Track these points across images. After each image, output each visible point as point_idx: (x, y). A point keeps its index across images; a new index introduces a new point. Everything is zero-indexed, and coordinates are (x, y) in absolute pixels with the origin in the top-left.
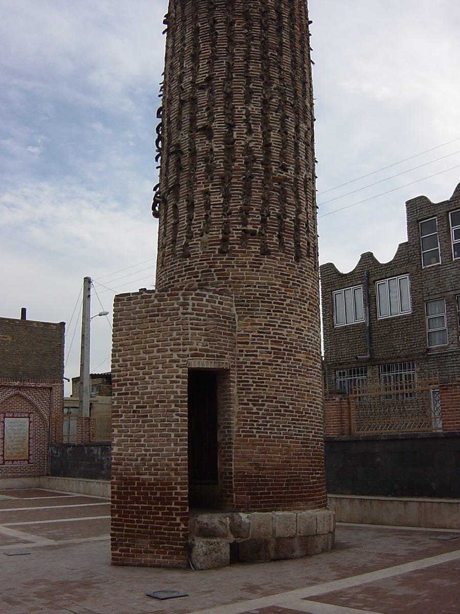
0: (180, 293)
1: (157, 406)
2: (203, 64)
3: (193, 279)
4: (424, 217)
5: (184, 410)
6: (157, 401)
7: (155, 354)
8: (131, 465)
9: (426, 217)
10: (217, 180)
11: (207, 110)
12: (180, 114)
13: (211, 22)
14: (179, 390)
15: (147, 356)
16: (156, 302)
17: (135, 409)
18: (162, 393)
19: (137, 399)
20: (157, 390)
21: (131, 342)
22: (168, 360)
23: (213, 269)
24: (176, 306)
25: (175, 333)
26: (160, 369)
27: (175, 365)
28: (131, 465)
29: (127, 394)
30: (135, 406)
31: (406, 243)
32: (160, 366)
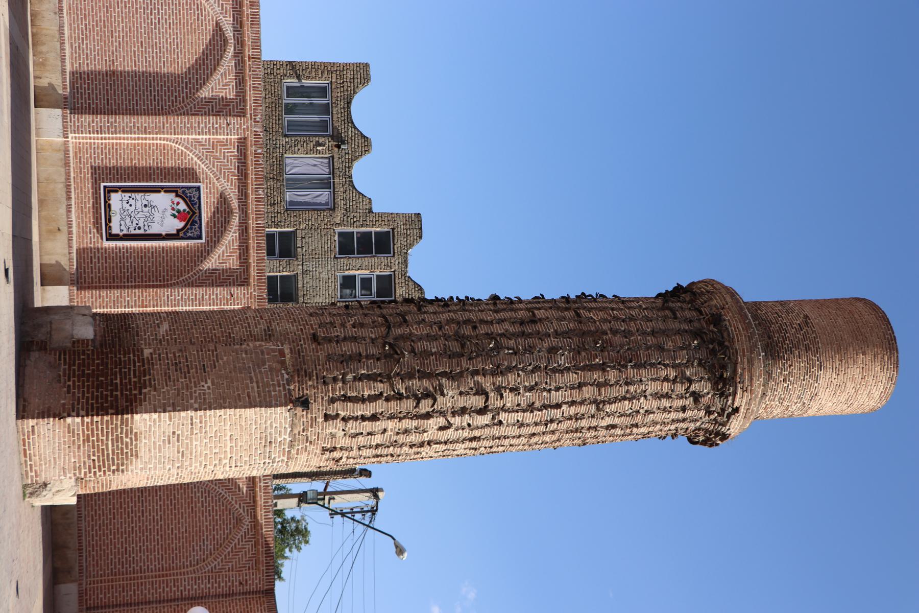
0: (285, 459)
1: (178, 452)
3: (302, 427)
4: (396, 238)
5: (173, 481)
6: (183, 451)
7: (229, 444)
8: (121, 433)
9: (396, 241)
10: (395, 438)
11: (469, 425)
13: (561, 419)
14: (193, 468)
15: (228, 438)
16: (279, 440)
17: (177, 433)
18: (191, 454)
19: (186, 434)
20: (194, 451)
21: (243, 424)
22: (223, 456)
23: (308, 444)
24: (273, 456)
25: (247, 459)
26: (214, 451)
27: (217, 462)
28: (121, 433)
29: (192, 424)
30: (180, 432)
32: (217, 451)
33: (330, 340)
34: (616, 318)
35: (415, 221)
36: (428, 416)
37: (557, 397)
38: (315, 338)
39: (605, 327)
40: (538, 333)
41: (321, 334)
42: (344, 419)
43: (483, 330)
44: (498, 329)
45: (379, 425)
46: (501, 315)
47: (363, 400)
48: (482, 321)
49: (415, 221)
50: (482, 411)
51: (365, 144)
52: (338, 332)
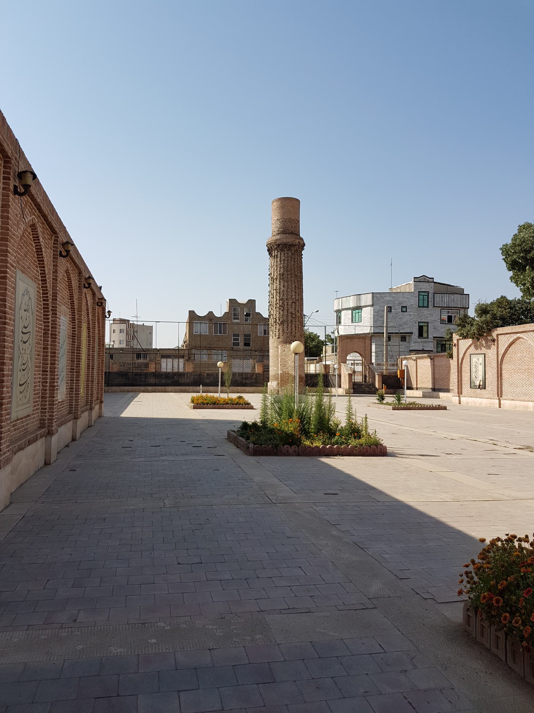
2: (297, 296)
12: (292, 304)
31: (228, 312)
33: (279, 335)
34: (276, 270)
35: (230, 300)
36: (296, 315)
37: (293, 286)
38: (278, 338)
39: (279, 273)
40: (279, 289)
41: (277, 337)
42: (295, 333)
43: (278, 301)
44: (278, 298)
45: (297, 326)
46: (275, 297)
47: (292, 329)
48: (276, 301)
49: (230, 300)
50: (295, 303)
51: (211, 313)
52: (277, 334)
